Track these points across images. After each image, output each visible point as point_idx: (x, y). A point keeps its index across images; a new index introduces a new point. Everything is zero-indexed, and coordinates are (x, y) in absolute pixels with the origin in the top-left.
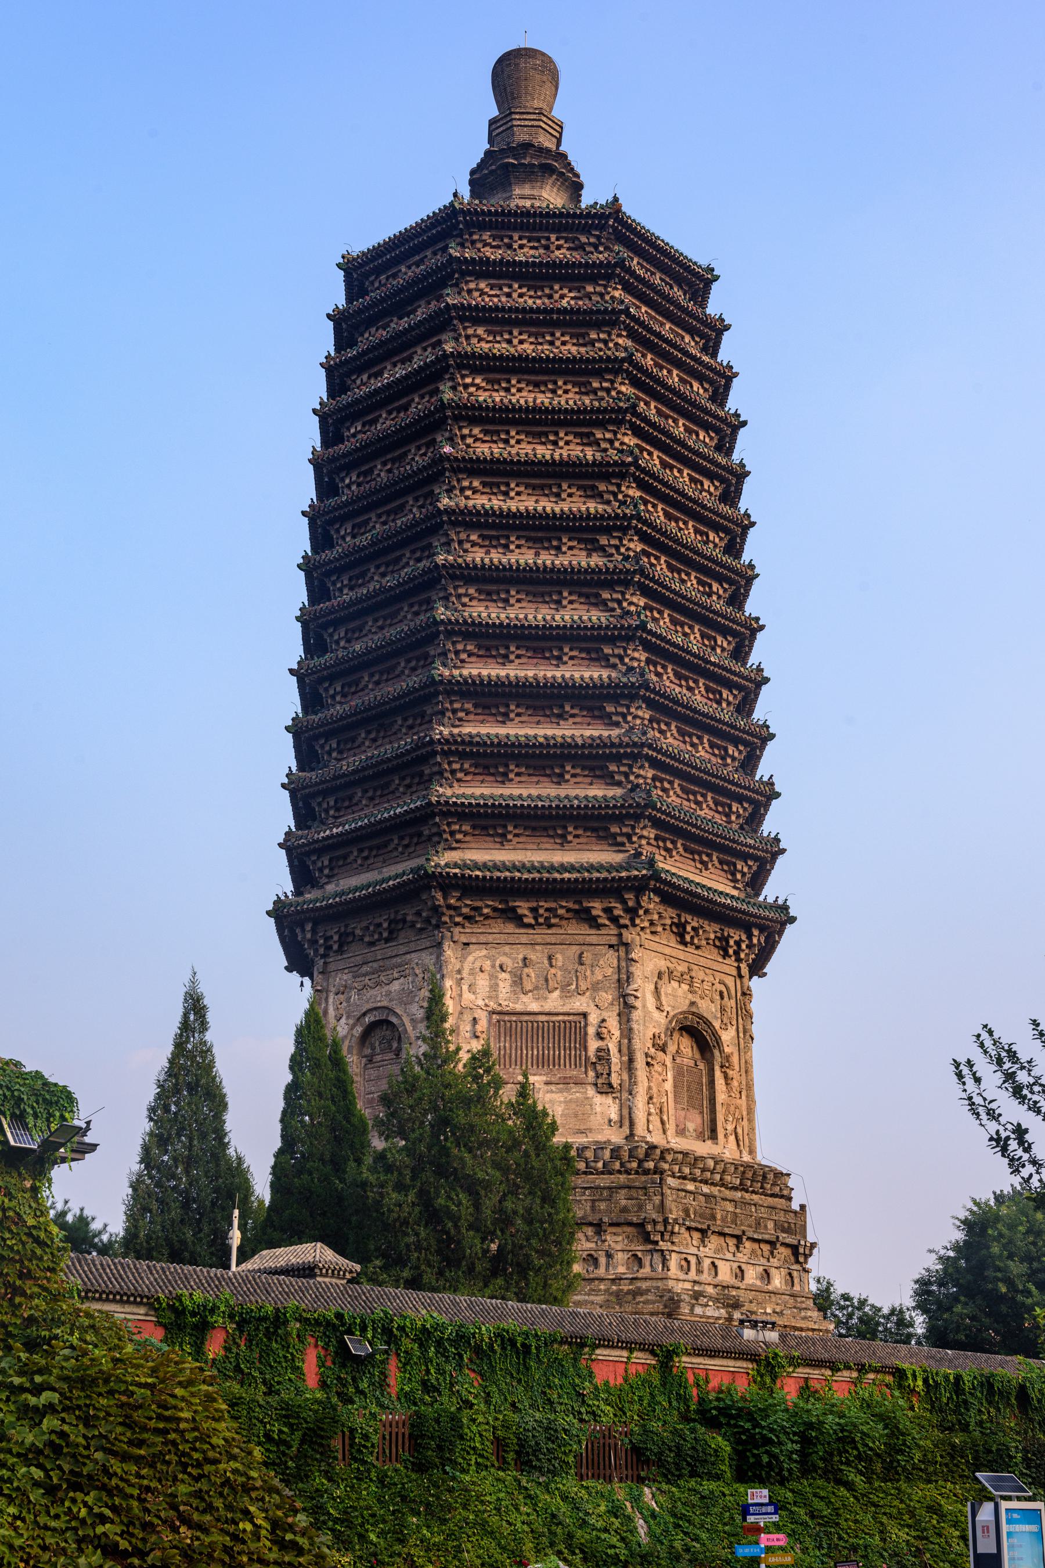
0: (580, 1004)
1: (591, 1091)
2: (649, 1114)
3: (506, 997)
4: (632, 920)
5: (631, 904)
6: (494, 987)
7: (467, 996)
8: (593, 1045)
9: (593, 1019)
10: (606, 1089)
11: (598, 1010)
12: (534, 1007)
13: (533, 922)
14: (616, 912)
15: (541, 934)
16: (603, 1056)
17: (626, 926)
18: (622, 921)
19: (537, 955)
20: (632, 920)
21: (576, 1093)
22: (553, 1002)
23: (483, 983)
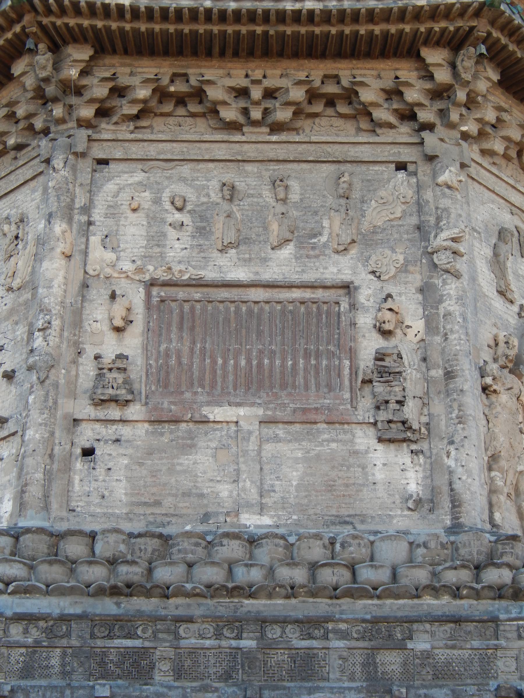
0: (338, 268)
1: (365, 439)
2: (492, 491)
3: (179, 252)
4: (443, 113)
5: (443, 76)
6: (157, 240)
7: (99, 255)
8: (369, 345)
9: (368, 293)
10: (398, 433)
11: (379, 289)
12: (241, 274)
13: (241, 119)
14: (412, 95)
15: (254, 142)
16: (386, 369)
17: (430, 127)
18: (424, 116)
19: (251, 181)
20: (443, 113)
21: (328, 442)
22: (282, 263)
23: (133, 233)
